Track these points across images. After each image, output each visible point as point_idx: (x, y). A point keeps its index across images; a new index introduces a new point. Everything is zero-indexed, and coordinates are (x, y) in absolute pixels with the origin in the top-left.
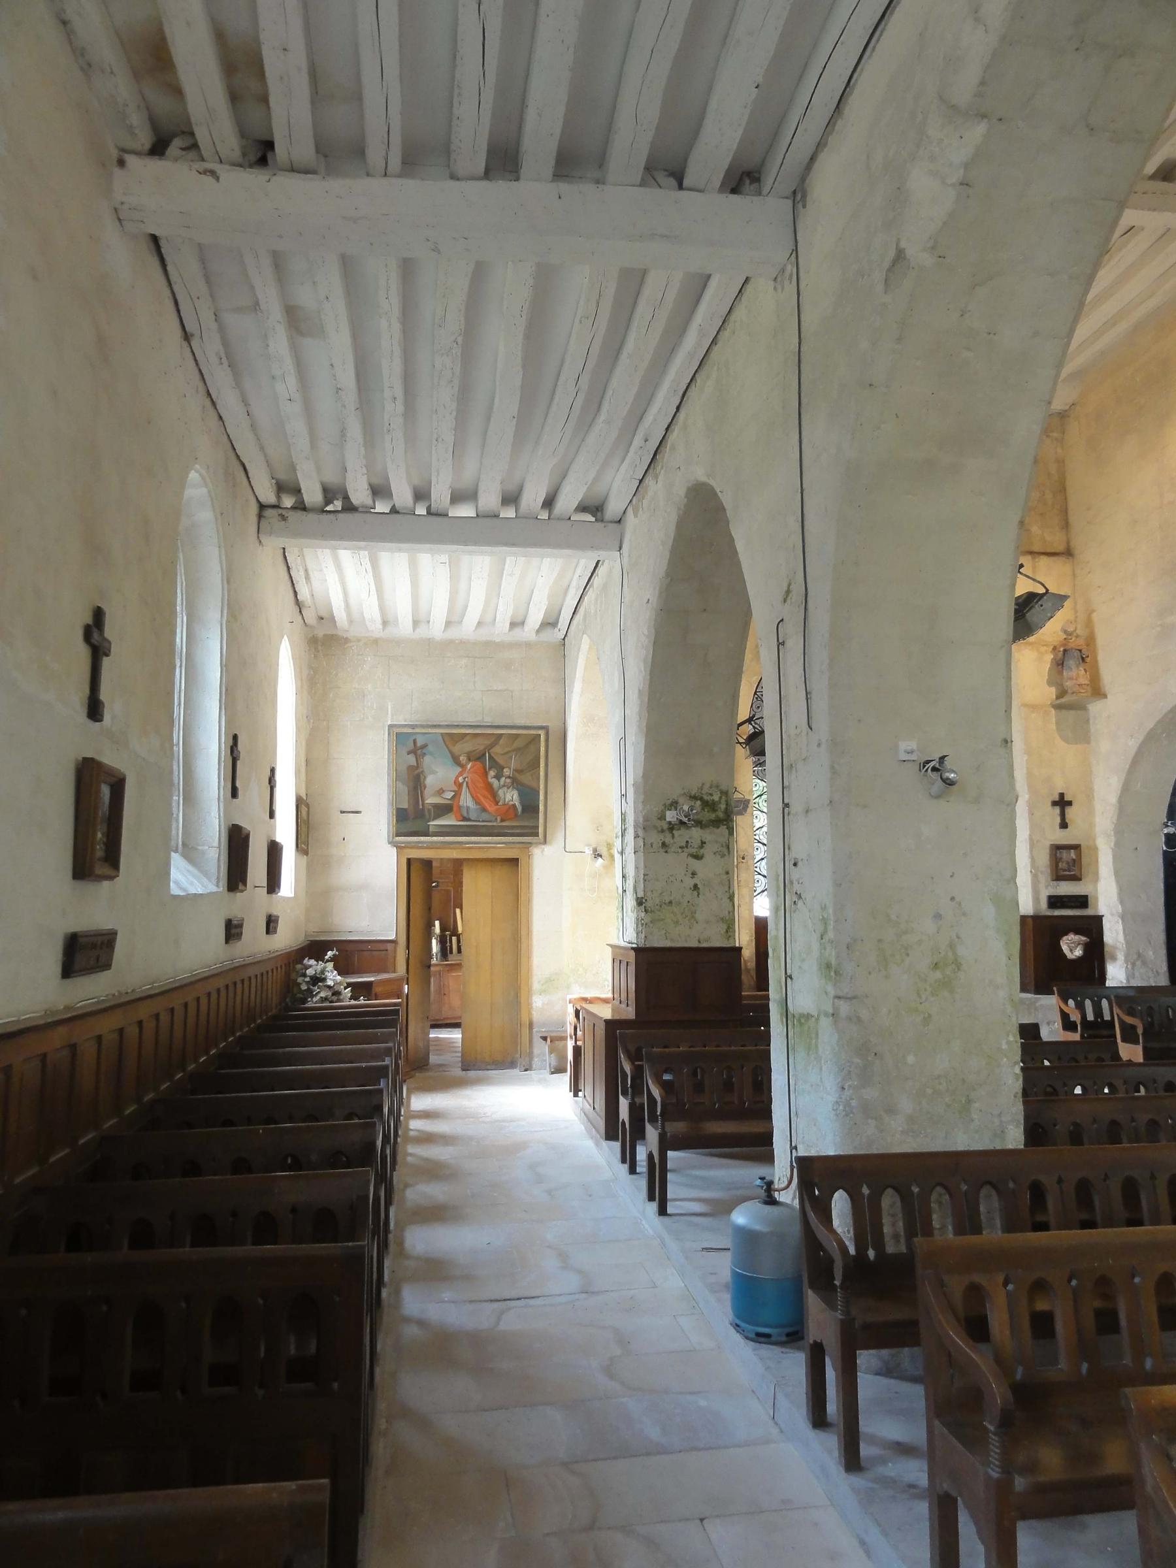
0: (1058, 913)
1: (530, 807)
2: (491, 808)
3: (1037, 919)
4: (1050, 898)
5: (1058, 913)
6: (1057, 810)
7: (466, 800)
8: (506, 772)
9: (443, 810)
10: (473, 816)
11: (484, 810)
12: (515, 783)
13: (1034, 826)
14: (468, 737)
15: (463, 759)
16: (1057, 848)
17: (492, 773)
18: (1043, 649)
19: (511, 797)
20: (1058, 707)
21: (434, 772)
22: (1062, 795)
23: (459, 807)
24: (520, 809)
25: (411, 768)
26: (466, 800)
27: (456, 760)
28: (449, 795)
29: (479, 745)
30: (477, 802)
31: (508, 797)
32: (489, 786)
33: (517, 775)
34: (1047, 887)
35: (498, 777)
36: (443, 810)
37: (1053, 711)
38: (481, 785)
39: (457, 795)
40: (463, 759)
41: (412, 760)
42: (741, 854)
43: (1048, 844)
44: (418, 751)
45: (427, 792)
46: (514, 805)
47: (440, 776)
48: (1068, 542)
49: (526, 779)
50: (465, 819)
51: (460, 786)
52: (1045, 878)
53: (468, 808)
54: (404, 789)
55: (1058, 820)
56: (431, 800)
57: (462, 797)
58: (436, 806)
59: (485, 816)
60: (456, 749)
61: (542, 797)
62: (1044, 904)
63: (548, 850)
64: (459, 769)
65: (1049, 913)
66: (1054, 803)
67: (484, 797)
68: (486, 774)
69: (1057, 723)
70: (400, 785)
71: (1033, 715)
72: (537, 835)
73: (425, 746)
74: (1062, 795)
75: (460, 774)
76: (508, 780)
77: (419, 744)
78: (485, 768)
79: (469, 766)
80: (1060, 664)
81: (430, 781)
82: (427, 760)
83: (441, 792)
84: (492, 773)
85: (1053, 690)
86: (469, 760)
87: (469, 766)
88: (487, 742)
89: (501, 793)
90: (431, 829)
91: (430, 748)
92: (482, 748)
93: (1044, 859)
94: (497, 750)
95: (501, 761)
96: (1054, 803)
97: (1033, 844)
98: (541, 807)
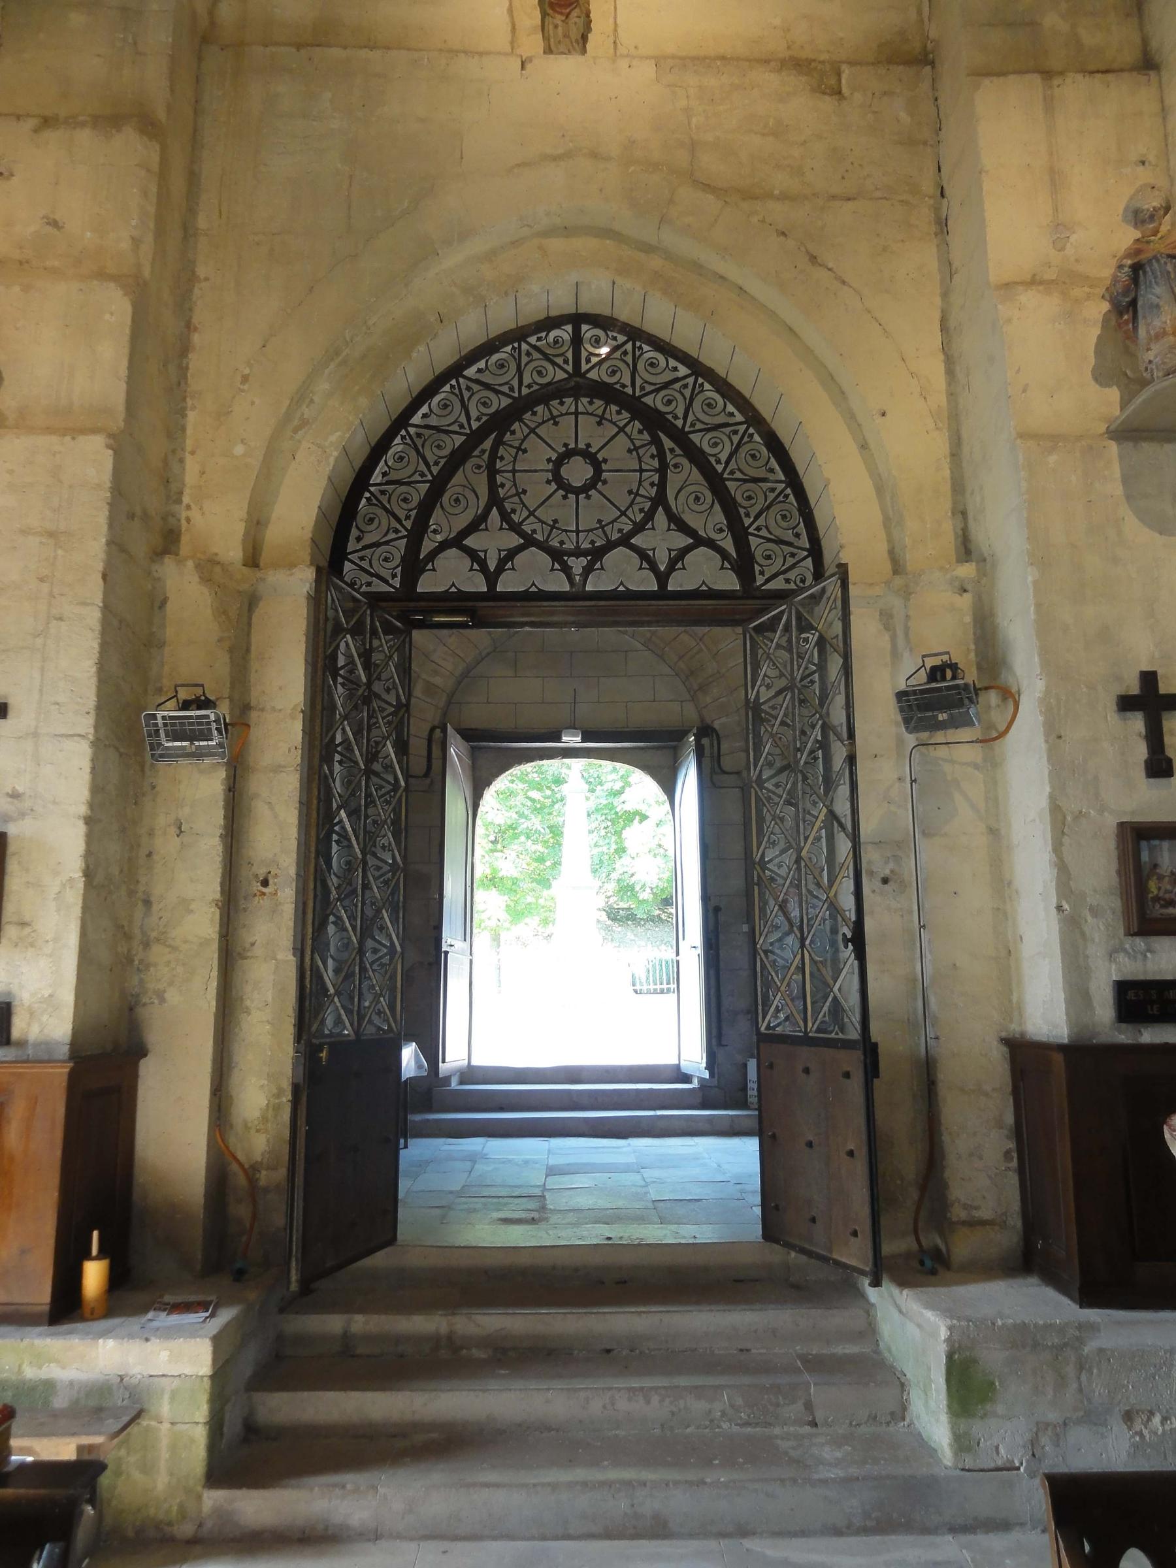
0: (1150, 1035)
3: (1081, 1055)
4: (1123, 988)
5: (1150, 1035)
6: (1137, 723)
13: (1062, 770)
16: (1137, 836)
18: (1077, 292)
20: (1128, 433)
22: (1149, 679)
34: (1111, 955)
37: (1113, 447)
42: (262, 872)
43: (1111, 822)
48: (1145, 42)
52: (1104, 927)
55: (1141, 751)
62: (1104, 1010)
65: (1124, 1036)
66: (1126, 704)
69: (1125, 480)
71: (1053, 459)
74: (1149, 679)
80: (1127, 306)
85: (1114, 394)
93: (1099, 868)
96: (1126, 704)
97: (1061, 822)
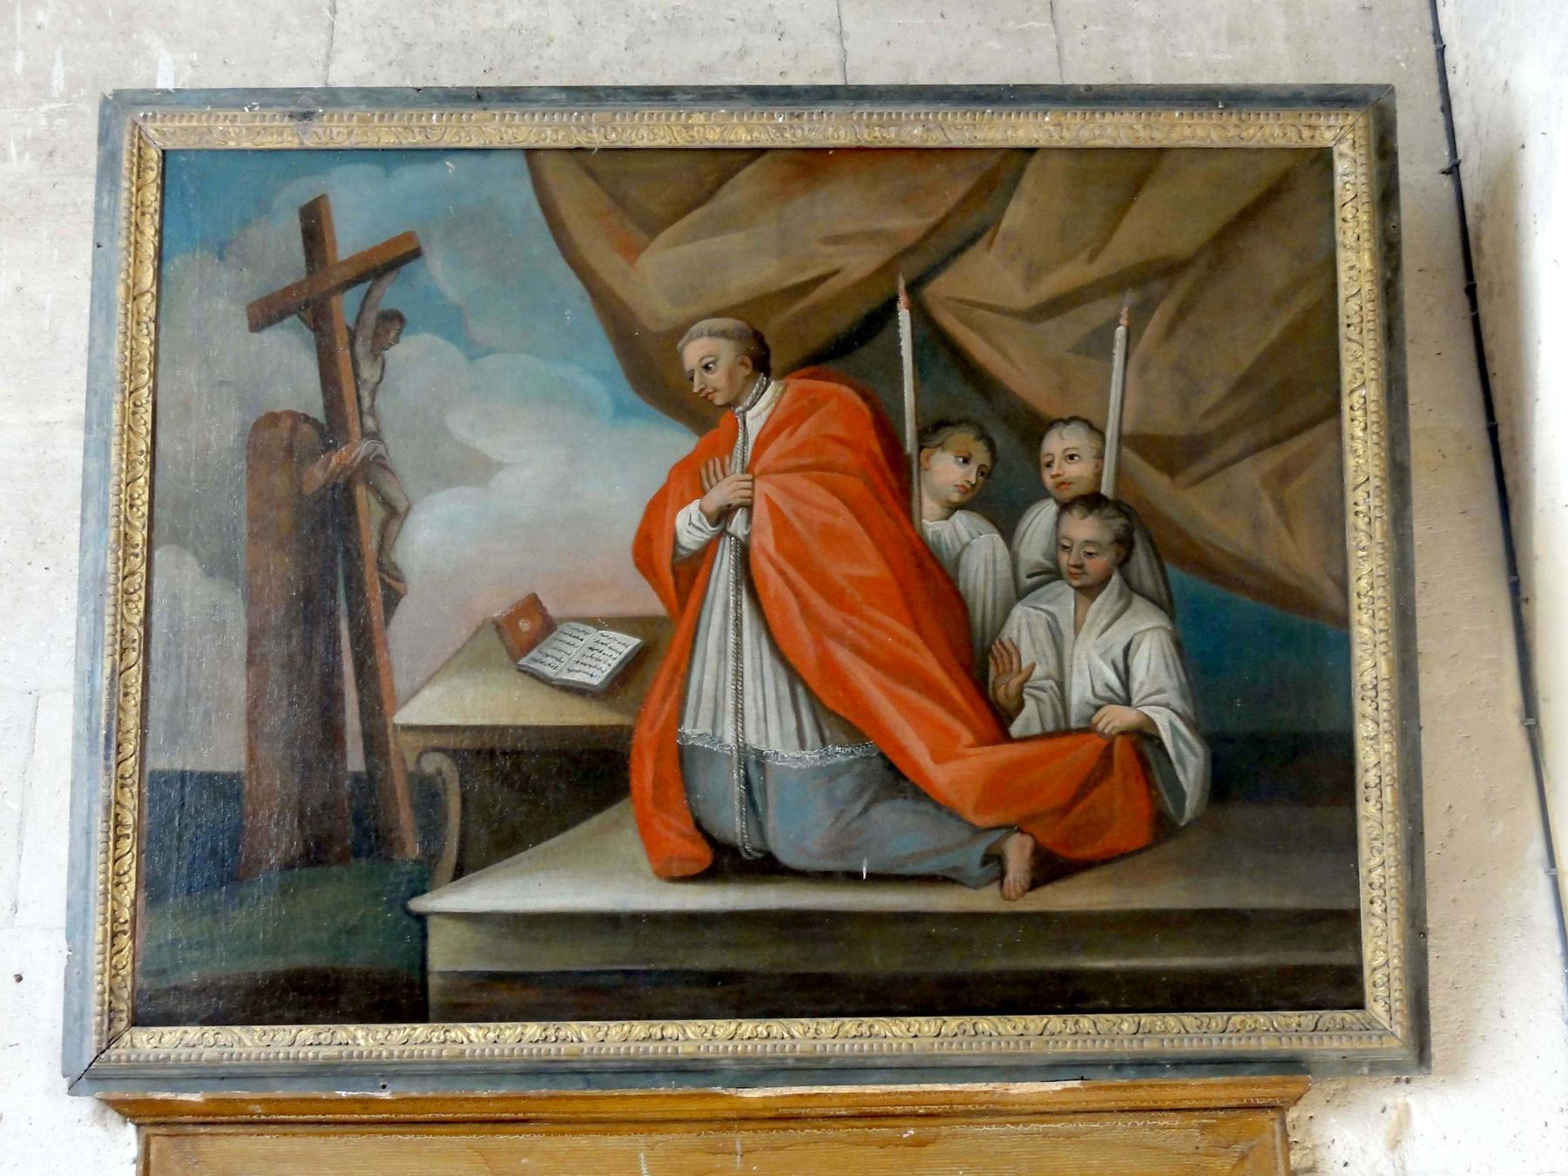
1: (1279, 751)
2: (957, 767)
7: (739, 702)
8: (1068, 455)
9: (559, 781)
10: (797, 833)
11: (894, 778)
12: (1143, 547)
14: (742, 189)
15: (707, 355)
17: (946, 471)
19: (1111, 662)
21: (476, 470)
23: (684, 758)
24: (1190, 767)
25: (275, 441)
26: (739, 702)
27: (651, 372)
28: (596, 656)
29: (841, 242)
30: (830, 709)
31: (1090, 670)
32: (931, 581)
33: (1154, 483)
35: (999, 503)
36: (559, 781)
38: (859, 565)
39: (657, 658)
40: (707, 355)
41: (287, 369)
44: (339, 296)
45: (407, 638)
46: (1144, 738)
47: (524, 498)
49: (1224, 510)
50: (727, 862)
51: (688, 575)
53: (753, 764)
54: (208, 612)
56: (444, 697)
57: (707, 673)
58: (490, 756)
59: (899, 833)
60: (658, 276)
61: (1370, 662)
63: (1429, 1107)
64: (679, 442)
67: (897, 670)
68: (898, 475)
70: (182, 578)
72: (1343, 987)
73: (396, 258)
75: (690, 478)
76: (1084, 528)
77: (351, 236)
78: (886, 427)
79: (756, 418)
81: (446, 544)
82: (414, 370)
83: (523, 630)
84: (946, 471)
86: (761, 363)
87: (756, 418)
88: (907, 224)
89: (1025, 630)
90: (446, 955)
91: (439, 271)
92: (859, 263)
94: (986, 279)
95: (1017, 363)
98: (1374, 752)
